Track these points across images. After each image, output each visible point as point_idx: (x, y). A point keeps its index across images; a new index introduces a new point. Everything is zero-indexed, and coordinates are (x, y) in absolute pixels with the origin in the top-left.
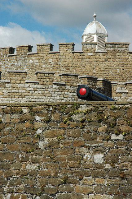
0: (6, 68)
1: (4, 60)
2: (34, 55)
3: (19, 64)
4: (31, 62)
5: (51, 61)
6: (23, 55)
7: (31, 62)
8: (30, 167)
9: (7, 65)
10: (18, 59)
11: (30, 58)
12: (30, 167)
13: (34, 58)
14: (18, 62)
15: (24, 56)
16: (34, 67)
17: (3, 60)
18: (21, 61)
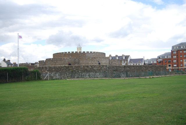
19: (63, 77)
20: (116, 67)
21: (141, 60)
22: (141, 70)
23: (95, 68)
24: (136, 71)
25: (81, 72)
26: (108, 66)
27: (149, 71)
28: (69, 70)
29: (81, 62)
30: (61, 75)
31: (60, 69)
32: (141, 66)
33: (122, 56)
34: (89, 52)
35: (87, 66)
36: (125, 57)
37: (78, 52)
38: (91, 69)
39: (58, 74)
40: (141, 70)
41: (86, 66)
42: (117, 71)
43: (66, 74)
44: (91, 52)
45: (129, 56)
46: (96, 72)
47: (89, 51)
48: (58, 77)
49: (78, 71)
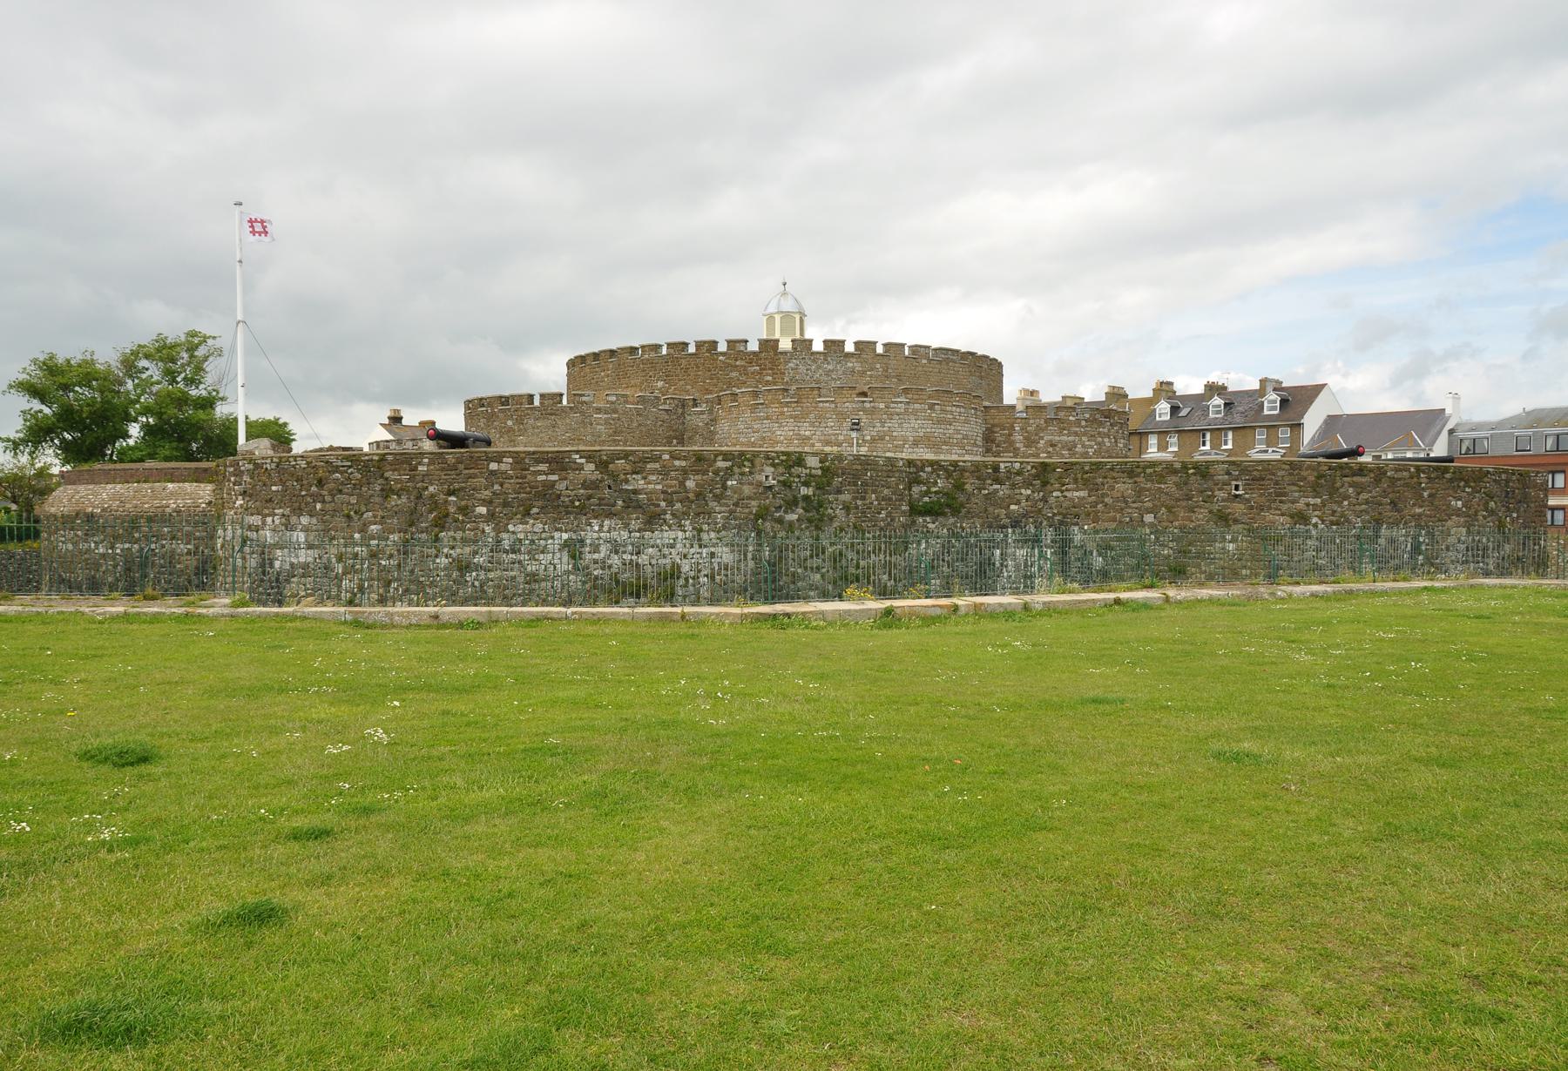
8: (1418, 510)
12: (1418, 510)
19: (340, 559)
20: (953, 470)
21: (1431, 419)
22: (1202, 515)
23: (637, 482)
24: (1149, 518)
25: (491, 516)
26: (813, 462)
27: (1302, 518)
28: (387, 492)
29: (723, 427)
30: (326, 532)
31: (320, 483)
32: (1203, 470)
33: (1261, 392)
34: (880, 350)
35: (559, 462)
36: (1284, 402)
37: (785, 345)
38: (594, 485)
39: (306, 530)
40: (1202, 515)
41: (539, 457)
42: (956, 512)
43: (363, 530)
45: (1318, 389)
46: (653, 520)
48: (304, 556)
49: (464, 510)
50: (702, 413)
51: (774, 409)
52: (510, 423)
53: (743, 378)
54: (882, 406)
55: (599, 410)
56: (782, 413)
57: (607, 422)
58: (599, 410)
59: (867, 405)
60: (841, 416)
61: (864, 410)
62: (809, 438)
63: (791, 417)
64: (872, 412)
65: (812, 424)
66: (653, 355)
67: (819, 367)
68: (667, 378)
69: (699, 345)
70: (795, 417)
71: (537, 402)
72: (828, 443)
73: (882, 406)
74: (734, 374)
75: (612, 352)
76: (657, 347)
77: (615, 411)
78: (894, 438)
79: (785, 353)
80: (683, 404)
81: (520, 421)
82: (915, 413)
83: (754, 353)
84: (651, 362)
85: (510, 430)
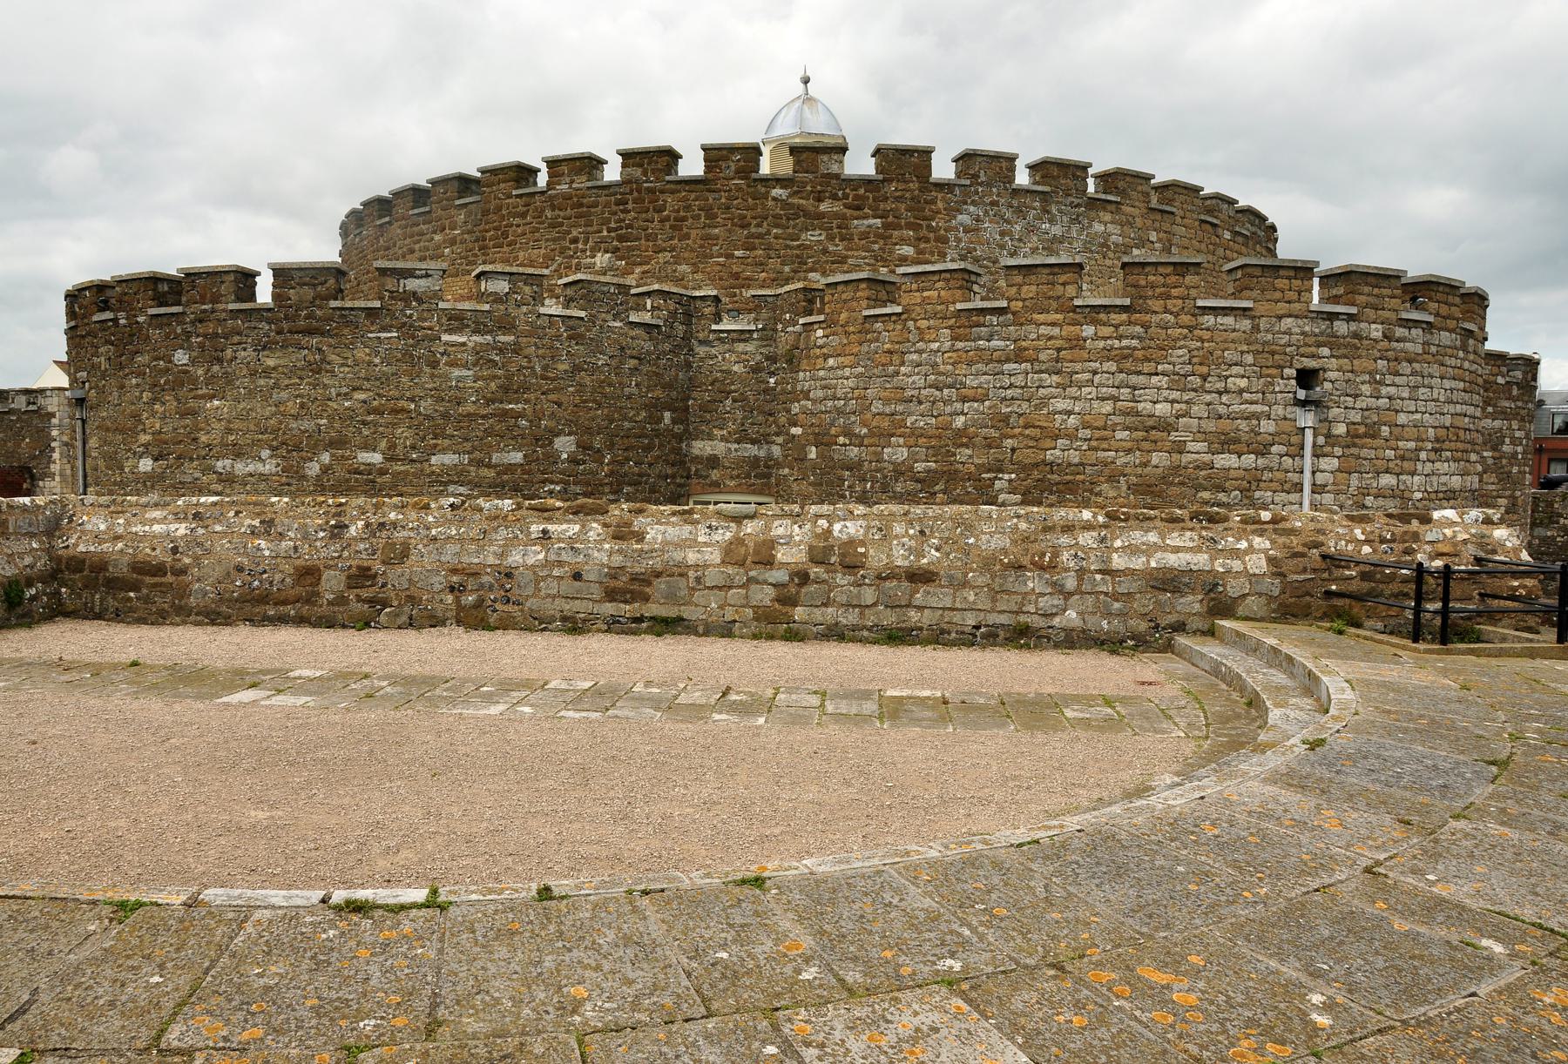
0: (1002, 234)
1: (993, 203)
2: (1110, 207)
3: (1056, 230)
4: (1098, 228)
5: (1153, 236)
6: (1071, 199)
7: (1098, 228)
9: (1008, 222)
10: (1054, 209)
11: (1093, 214)
13: (1108, 217)
14: (1051, 221)
15: (1077, 201)
16: (1108, 247)
17: (987, 200)
18: (1065, 219)
44: (1059, 175)
47: (1029, 149)
50: (743, 336)
51: (1046, 330)
52: (181, 357)
53: (838, 247)
54: (1376, 331)
55: (457, 321)
56: (1077, 343)
57: (480, 357)
58: (457, 321)
59: (1341, 327)
60: (1269, 358)
61: (1333, 341)
62: (1166, 426)
63: (1107, 355)
64: (1350, 348)
65: (1178, 381)
66: (581, 182)
67: (1031, 229)
68: (623, 244)
69: (715, 155)
70: (1123, 356)
71: (264, 292)
72: (1227, 443)
73: (1376, 331)
74: (813, 237)
75: (463, 183)
76: (591, 164)
77: (506, 325)
78: (1398, 432)
79: (942, 186)
80: (687, 309)
81: (212, 353)
82: (1438, 358)
83: (866, 182)
84: (579, 206)
85: (183, 379)
